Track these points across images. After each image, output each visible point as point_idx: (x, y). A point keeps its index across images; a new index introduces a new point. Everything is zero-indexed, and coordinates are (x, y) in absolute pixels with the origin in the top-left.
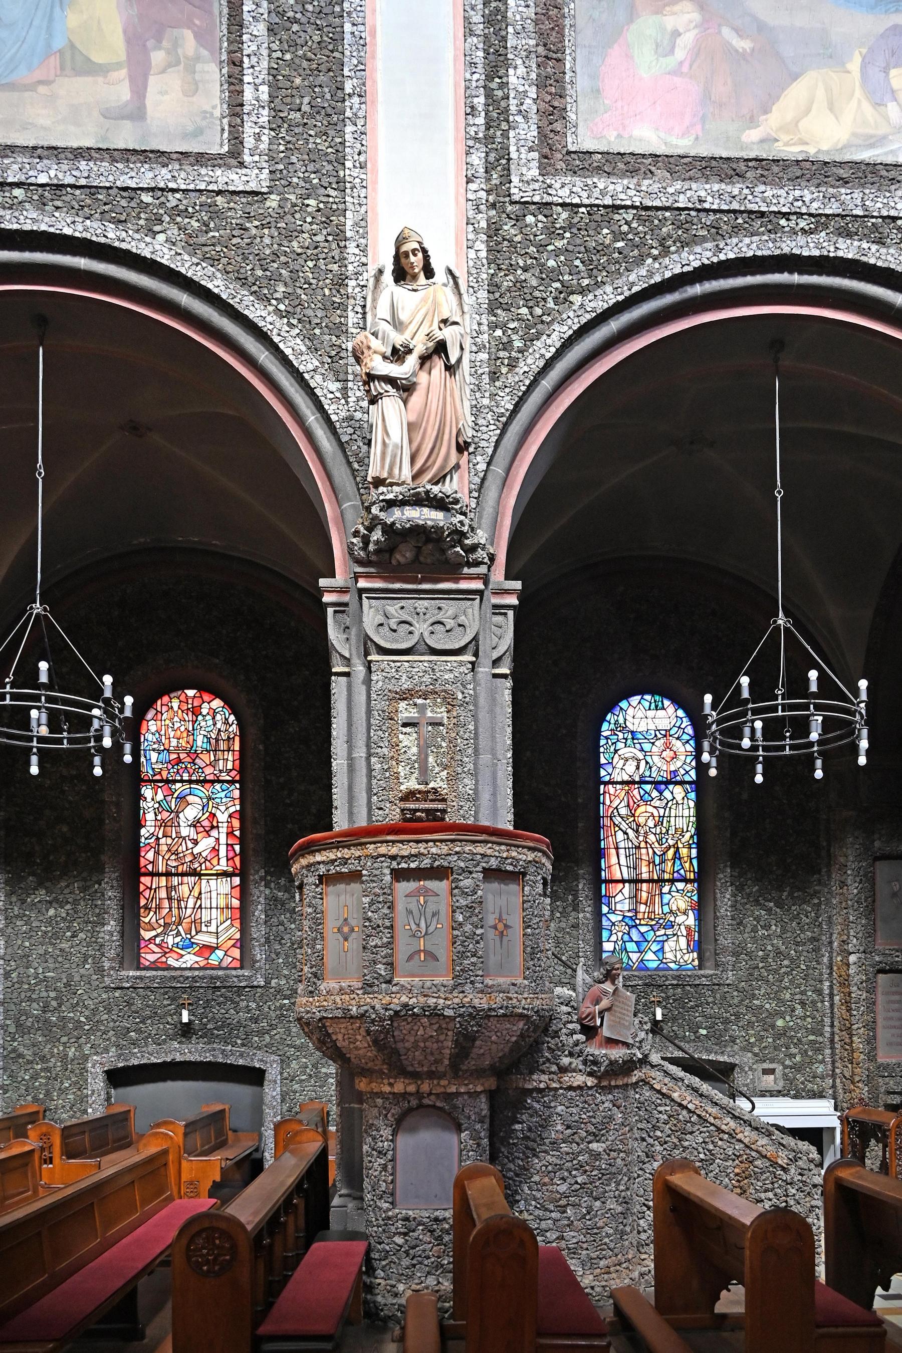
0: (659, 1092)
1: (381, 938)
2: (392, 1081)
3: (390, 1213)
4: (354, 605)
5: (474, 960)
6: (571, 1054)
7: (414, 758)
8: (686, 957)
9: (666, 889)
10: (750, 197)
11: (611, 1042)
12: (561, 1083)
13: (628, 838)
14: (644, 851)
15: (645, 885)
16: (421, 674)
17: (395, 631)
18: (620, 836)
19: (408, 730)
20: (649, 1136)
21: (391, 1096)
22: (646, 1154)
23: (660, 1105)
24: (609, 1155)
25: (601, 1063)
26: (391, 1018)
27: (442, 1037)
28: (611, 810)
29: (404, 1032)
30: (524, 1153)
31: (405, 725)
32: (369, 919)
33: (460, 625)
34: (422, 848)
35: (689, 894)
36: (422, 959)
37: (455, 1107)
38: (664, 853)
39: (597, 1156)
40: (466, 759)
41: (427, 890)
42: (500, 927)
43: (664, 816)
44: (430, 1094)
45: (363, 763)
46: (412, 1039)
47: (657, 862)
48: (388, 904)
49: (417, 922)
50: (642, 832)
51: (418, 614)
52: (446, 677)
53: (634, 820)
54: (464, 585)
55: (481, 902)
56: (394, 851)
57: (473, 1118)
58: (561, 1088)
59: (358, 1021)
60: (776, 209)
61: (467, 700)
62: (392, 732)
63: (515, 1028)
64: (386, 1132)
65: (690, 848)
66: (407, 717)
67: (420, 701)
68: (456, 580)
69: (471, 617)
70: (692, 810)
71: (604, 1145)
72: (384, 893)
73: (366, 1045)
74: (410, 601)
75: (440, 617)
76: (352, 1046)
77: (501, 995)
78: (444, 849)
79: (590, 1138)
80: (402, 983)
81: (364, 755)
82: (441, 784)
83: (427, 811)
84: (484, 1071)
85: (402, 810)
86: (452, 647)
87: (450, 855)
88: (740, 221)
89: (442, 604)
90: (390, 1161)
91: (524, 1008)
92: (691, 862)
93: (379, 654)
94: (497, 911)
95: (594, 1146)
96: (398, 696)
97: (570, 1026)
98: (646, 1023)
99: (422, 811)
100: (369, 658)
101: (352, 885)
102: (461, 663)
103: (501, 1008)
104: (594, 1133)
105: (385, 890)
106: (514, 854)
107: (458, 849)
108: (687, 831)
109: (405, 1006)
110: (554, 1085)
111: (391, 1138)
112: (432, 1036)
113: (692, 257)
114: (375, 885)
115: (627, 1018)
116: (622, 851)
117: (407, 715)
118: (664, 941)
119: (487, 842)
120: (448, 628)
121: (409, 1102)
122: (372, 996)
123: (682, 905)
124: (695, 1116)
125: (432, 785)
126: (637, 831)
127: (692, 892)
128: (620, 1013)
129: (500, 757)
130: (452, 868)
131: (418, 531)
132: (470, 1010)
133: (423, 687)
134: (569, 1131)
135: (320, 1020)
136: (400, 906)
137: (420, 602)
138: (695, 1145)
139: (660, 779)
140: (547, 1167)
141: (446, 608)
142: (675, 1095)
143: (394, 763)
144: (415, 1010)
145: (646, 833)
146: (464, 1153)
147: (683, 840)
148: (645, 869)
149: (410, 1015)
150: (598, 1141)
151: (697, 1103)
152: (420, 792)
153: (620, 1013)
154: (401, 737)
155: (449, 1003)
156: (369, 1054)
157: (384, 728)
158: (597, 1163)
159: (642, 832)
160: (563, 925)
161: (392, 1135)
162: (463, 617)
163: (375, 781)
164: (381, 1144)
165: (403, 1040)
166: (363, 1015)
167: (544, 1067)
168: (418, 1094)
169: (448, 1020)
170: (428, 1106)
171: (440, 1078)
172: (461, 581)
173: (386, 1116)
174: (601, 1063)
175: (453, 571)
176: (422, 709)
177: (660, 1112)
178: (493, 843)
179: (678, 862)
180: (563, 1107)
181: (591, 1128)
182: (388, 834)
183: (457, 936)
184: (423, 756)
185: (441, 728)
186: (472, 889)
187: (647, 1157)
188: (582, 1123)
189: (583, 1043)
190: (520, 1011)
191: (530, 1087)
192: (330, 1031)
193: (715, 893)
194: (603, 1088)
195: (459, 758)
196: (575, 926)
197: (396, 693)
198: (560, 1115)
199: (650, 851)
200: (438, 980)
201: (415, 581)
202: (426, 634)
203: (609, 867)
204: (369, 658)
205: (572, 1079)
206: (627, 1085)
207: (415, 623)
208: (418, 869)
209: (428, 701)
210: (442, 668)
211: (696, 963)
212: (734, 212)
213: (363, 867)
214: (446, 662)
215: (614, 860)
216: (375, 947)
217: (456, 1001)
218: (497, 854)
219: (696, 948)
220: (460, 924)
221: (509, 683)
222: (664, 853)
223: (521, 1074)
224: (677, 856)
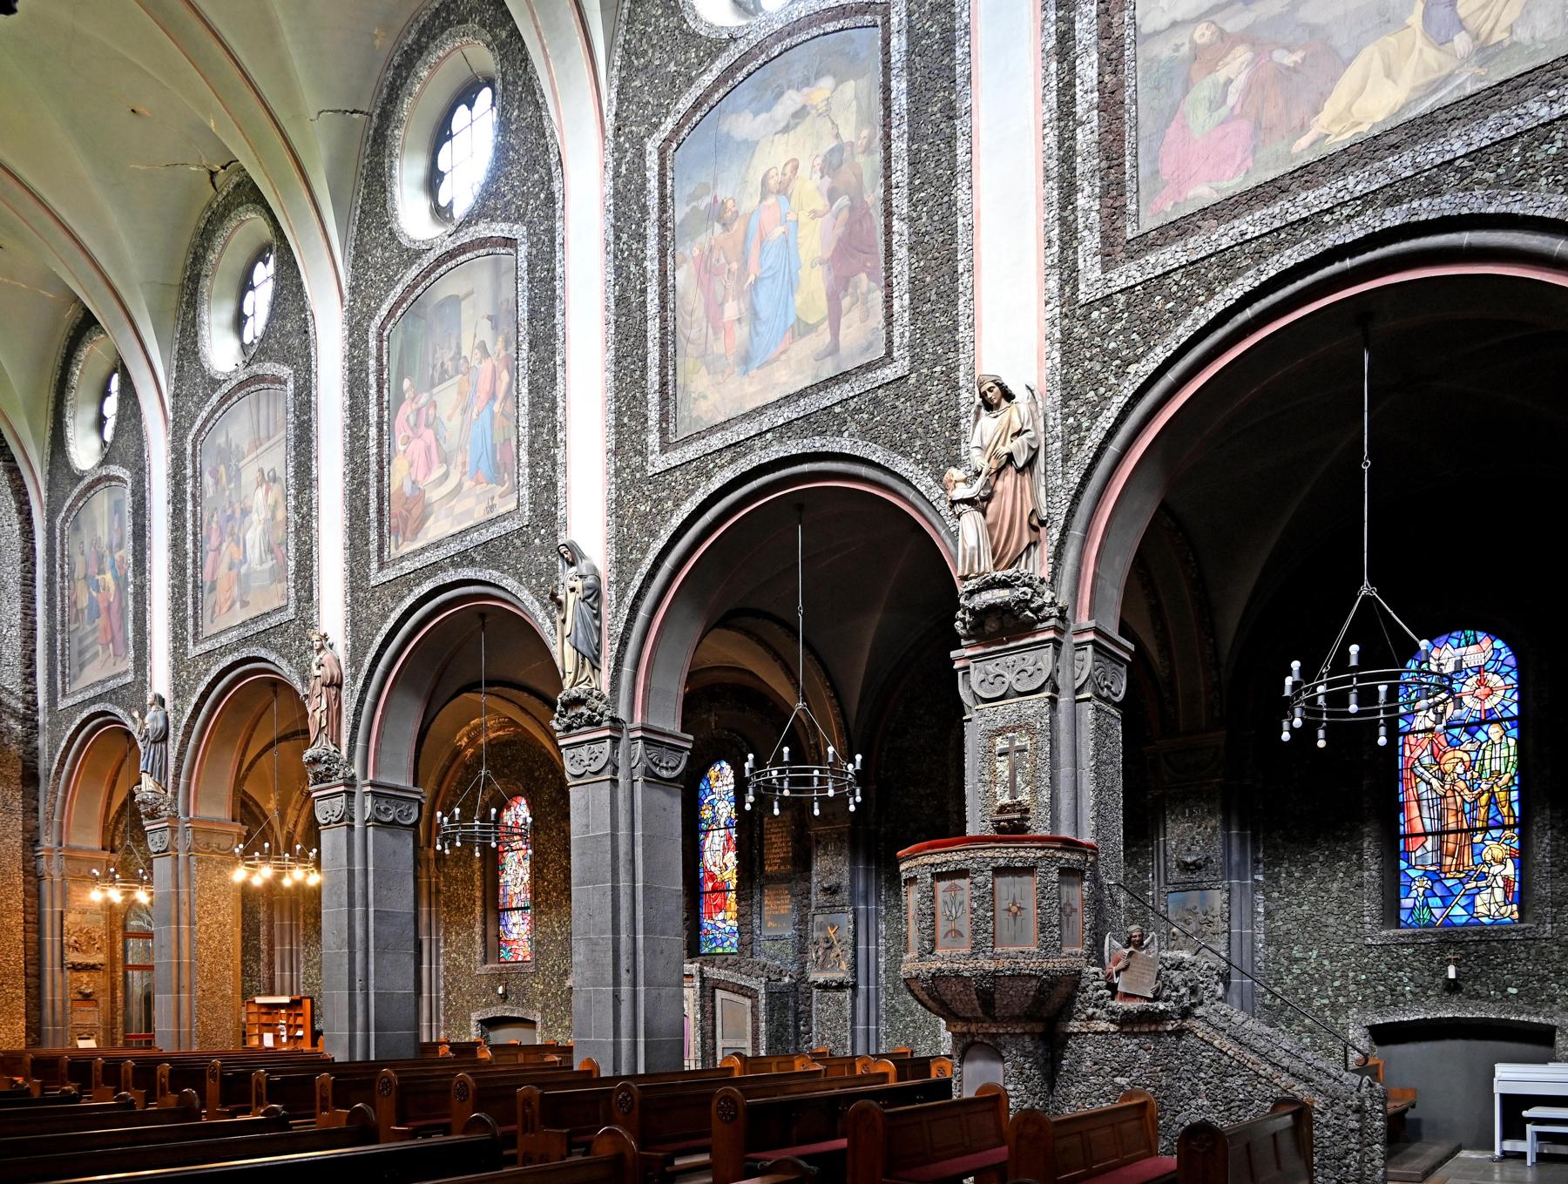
0: (1202, 1039)
8: (1503, 910)
9: (1478, 838)
10: (1291, 210)
11: (1127, 996)
14: (1451, 800)
15: (1452, 837)
18: (1423, 787)
19: (1002, 758)
34: (948, 857)
37: (998, 1044)
42: (1014, 909)
54: (1039, 638)
56: (932, 860)
60: (1317, 210)
68: (1034, 635)
70: (1512, 749)
78: (962, 856)
83: (1008, 821)
84: (1018, 1017)
88: (1283, 236)
89: (1025, 655)
102: (1040, 700)
106: (1022, 854)
109: (939, 969)
110: (1085, 1030)
113: (1234, 291)
116: (1425, 803)
118: (1475, 895)
126: (1442, 780)
127: (1512, 837)
131: (992, 609)
139: (1472, 720)
148: (1452, 819)
160: (1347, 885)
175: (1029, 628)
194: (1126, 1033)
196: (1360, 885)
199: (1459, 799)
203: (1410, 820)
208: (947, 872)
211: (1516, 915)
212: (1276, 230)
215: (1415, 813)
219: (1516, 899)
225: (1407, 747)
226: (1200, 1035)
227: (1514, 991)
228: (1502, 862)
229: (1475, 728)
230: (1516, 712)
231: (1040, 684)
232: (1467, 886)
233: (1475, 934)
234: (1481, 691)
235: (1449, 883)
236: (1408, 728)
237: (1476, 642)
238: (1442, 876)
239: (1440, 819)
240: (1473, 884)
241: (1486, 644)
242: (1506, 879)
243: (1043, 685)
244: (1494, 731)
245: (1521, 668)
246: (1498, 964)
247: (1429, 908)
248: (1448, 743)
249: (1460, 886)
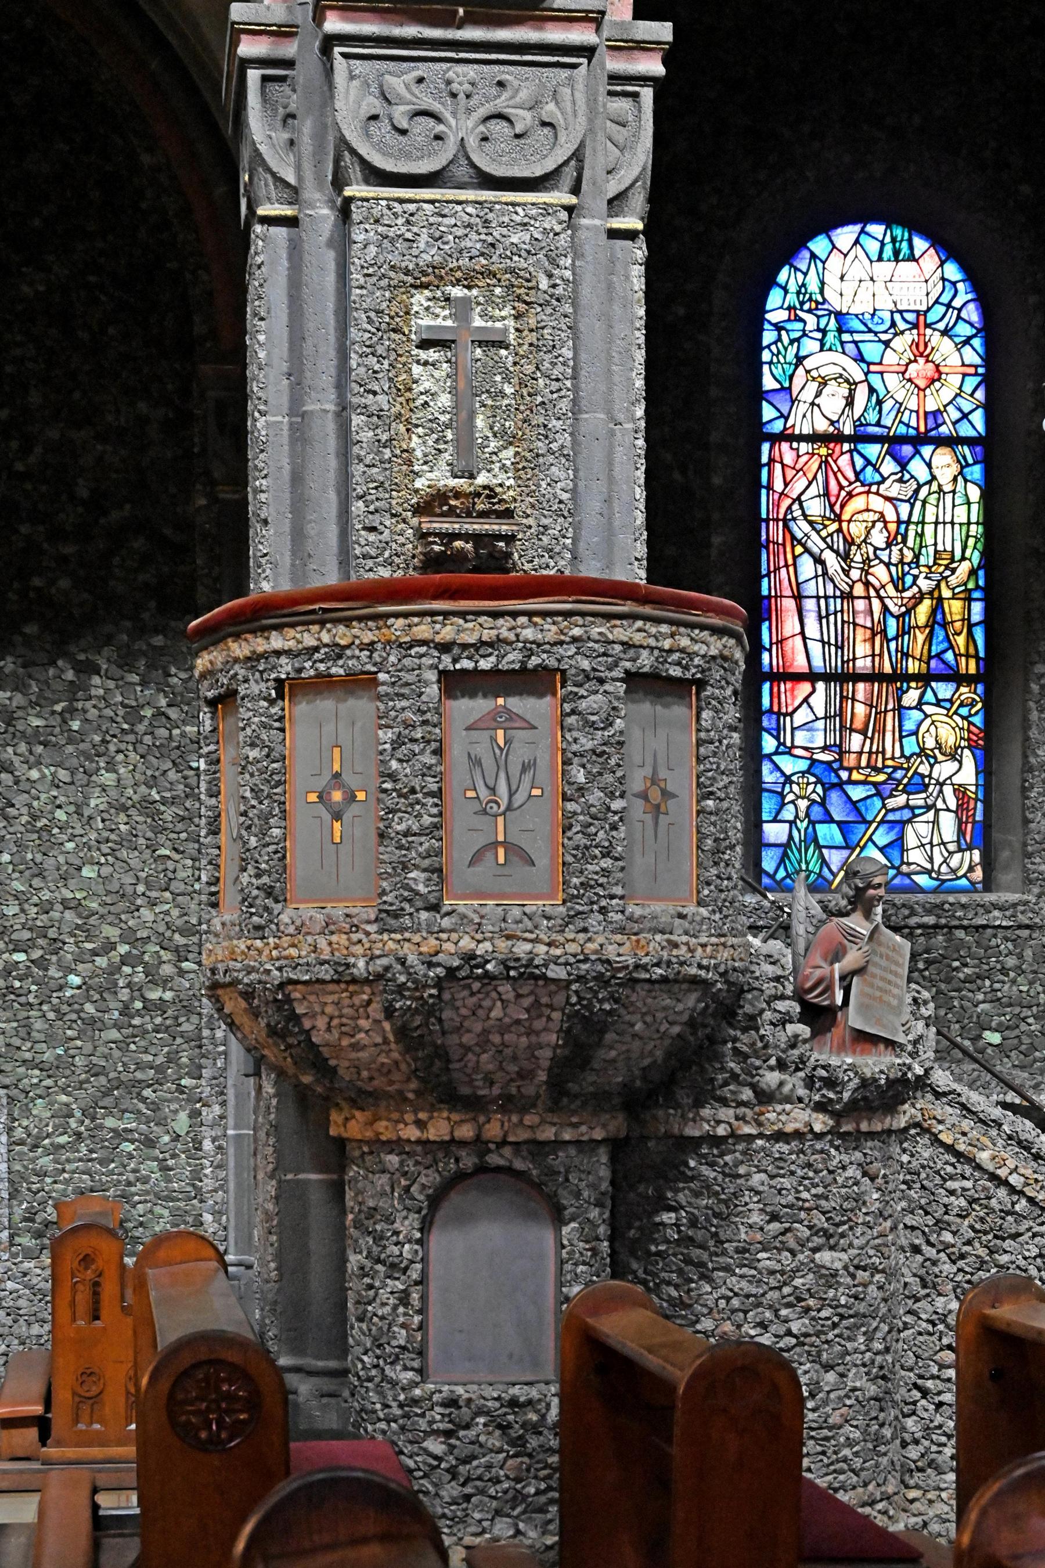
0: (950, 1149)
1: (419, 816)
2: (422, 1116)
3: (417, 1392)
4: (308, 69)
5: (606, 863)
6: (781, 1065)
7: (444, 418)
9: (911, 697)
11: (864, 1039)
12: (760, 1124)
13: (825, 573)
14: (860, 605)
16: (460, 232)
17: (403, 132)
18: (807, 567)
19: (432, 355)
20: (929, 1243)
21: (419, 1149)
22: (922, 1279)
23: (951, 1178)
24: (853, 1276)
25: (843, 1084)
26: (439, 983)
27: (539, 1024)
28: (787, 502)
29: (464, 1011)
30: (680, 1272)
31: (425, 344)
32: (392, 776)
33: (544, 124)
35: (964, 711)
36: (501, 860)
38: (908, 612)
39: (830, 1278)
40: (554, 423)
41: (511, 716)
42: (655, 795)
43: (908, 522)
44: (503, 1143)
45: (331, 426)
46: (478, 1027)
47: (892, 632)
48: (434, 745)
49: (491, 784)
50: (858, 558)
51: (454, 95)
52: (515, 239)
53: (840, 530)
54: (555, 35)
55: (621, 744)
56: (447, 633)
57: (586, 1194)
58: (761, 1136)
59: (367, 989)
61: (559, 291)
62: (397, 360)
63: (680, 1007)
64: (407, 1225)
65: (969, 600)
66: (429, 328)
67: (457, 292)
69: (568, 106)
71: (844, 1256)
72: (425, 723)
73: (379, 1040)
74: (438, 66)
75: (501, 103)
76: (345, 1042)
77: (658, 937)
78: (551, 630)
79: (818, 1241)
80: (462, 909)
81: (331, 407)
82: (502, 477)
83: (476, 538)
84: (606, 1095)
85: (422, 536)
86: (526, 173)
87: (561, 643)
90: (417, 1283)
91: (700, 967)
92: (970, 635)
93: (367, 182)
94: (649, 760)
95: (825, 1257)
96: (409, 279)
97: (782, 1006)
98: (925, 1002)
99: (466, 537)
100: (348, 192)
101: (351, 702)
102: (547, 209)
103: (657, 965)
104: (825, 1231)
105: (428, 716)
106: (685, 642)
107: (577, 632)
108: (963, 558)
110: (747, 1130)
111: (418, 1235)
112: (518, 1022)
114: (404, 703)
115: (896, 991)
116: (810, 605)
117: (426, 321)
119: (633, 617)
120: (519, 128)
121: (457, 1160)
122: (398, 936)
123: (949, 736)
124: (1024, 1201)
125: (482, 479)
126: (846, 557)
128: (883, 979)
129: (621, 417)
130: (563, 672)
132: (600, 968)
133: (464, 262)
134: (775, 1226)
135: (281, 986)
136: (457, 749)
137: (460, 68)
138: (1022, 1263)
140: (728, 1299)
141: (516, 83)
142: (984, 1157)
143: (402, 428)
144: (489, 967)
145: (867, 561)
146: (568, 1267)
147: (953, 580)
148: (862, 649)
149: (478, 978)
150: (832, 1248)
151: (1028, 1172)
152: (457, 495)
153: (883, 979)
154: (417, 370)
155: (558, 952)
156: (383, 1059)
157: (380, 350)
158: (831, 1293)
159: (858, 558)
161: (421, 1230)
162: (551, 106)
163: (361, 468)
164: (396, 1250)
165: (459, 1029)
166: (379, 977)
167: (726, 1092)
168: (479, 1145)
169: (553, 987)
170: (498, 1169)
171: (524, 1110)
172: (550, 25)
173: (407, 1189)
174: (843, 1084)
176: (462, 309)
177: (952, 1193)
178: (646, 618)
179: (940, 634)
180: (763, 1176)
181: (820, 1221)
182: (436, 597)
183: (575, 813)
184: (464, 415)
185: (503, 352)
186: (604, 716)
187: (924, 1286)
188: (801, 1209)
189: (805, 1041)
190: (693, 971)
191: (697, 1133)
192: (300, 1010)
193: (1027, 711)
194: (844, 1136)
195: (541, 420)
197: (407, 272)
198: (758, 1193)
199: (876, 604)
200: (533, 906)
201: (448, 21)
202: (472, 142)
203: (781, 642)
204: (348, 192)
205: (783, 1118)
206: (889, 1132)
207: (447, 115)
209: (475, 292)
210: (506, 219)
213: (381, 666)
214: (514, 204)
216: (407, 833)
217: (572, 948)
218: (652, 642)
220: (581, 789)
221: (639, 251)
222: (908, 612)
223: (677, 1106)
224: (937, 620)
225: (778, 466)
226: (946, 1138)
227: (995, 1038)
228: (954, 755)
229: (907, 450)
230: (981, 427)
231: (550, 165)
232: (891, 803)
233: (929, 912)
234: (919, 369)
235: (857, 793)
236: (778, 427)
237: (912, 258)
238: (844, 775)
239: (839, 647)
240: (901, 800)
241: (930, 261)
242: (960, 791)
243: (557, 171)
244: (944, 461)
245: (989, 330)
246: (967, 980)
247: (819, 847)
248: (857, 474)
249: (877, 803)
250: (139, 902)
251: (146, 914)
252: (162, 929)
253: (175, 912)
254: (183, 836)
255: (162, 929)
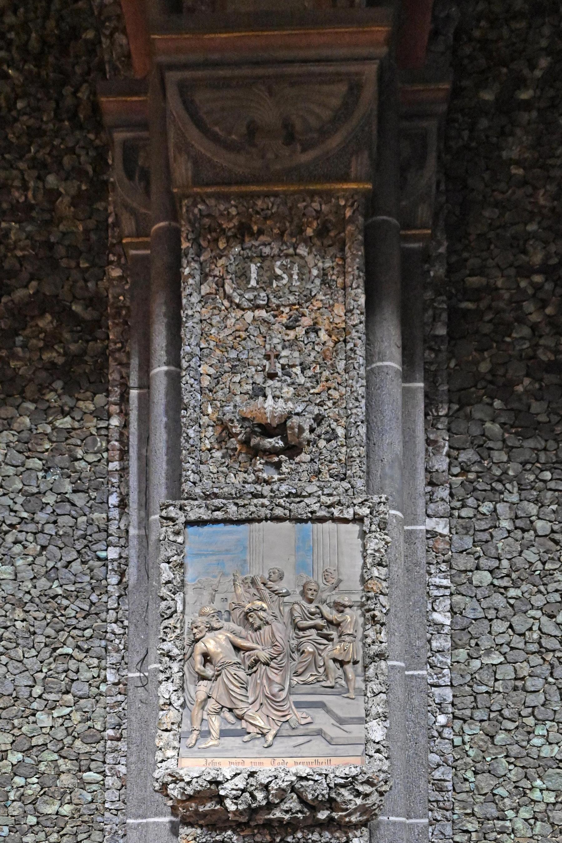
250: (35, 705)
251: (44, 719)
252: (60, 734)
253: (77, 717)
254: (88, 633)
255: (60, 734)
